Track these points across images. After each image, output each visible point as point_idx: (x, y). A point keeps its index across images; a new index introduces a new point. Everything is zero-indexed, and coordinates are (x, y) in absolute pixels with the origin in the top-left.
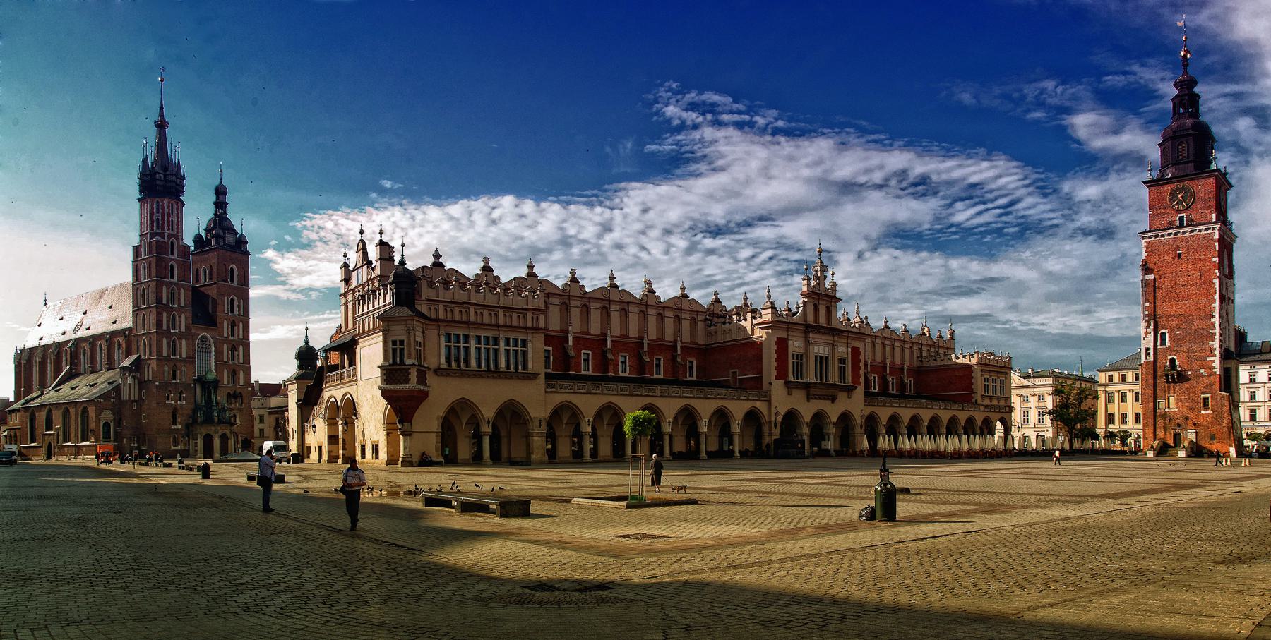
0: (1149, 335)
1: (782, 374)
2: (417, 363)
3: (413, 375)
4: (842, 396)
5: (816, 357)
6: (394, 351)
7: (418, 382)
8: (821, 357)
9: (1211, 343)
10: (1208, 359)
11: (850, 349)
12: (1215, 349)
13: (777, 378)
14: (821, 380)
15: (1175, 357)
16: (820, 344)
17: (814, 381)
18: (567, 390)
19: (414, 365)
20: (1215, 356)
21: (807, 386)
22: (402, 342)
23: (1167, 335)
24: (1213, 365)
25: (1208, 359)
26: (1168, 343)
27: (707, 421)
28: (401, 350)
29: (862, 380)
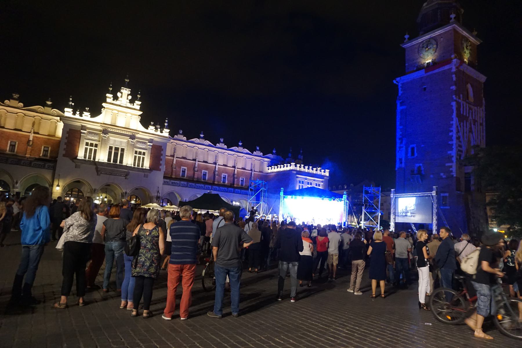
8: (117, 149)
9: (449, 152)
10: (447, 165)
12: (453, 156)
20: (452, 162)
24: (451, 169)
25: (447, 165)
26: (416, 155)
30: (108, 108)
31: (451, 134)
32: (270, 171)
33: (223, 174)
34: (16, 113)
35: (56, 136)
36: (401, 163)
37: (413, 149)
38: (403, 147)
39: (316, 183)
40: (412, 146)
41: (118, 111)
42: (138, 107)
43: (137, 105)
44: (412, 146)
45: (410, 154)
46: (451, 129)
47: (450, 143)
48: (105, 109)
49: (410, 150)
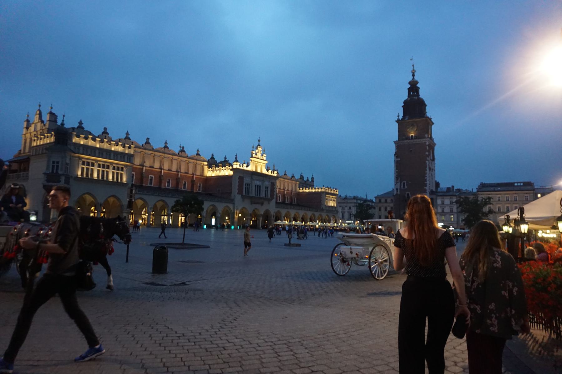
0: (398, 183)
1: (240, 192)
2: (65, 173)
3: (63, 179)
4: (266, 203)
5: (255, 186)
6: (53, 166)
7: (65, 183)
8: (258, 186)
9: (425, 188)
11: (270, 183)
12: (426, 190)
13: (238, 193)
14: (257, 195)
15: (409, 193)
16: (257, 180)
17: (254, 196)
18: (141, 193)
19: (63, 175)
21: (251, 198)
22: (58, 163)
23: (406, 184)
26: (406, 187)
27: (206, 211)
28: (57, 166)
29: (275, 197)
30: (254, 161)
31: (426, 178)
32: (301, 191)
33: (150, 176)
34: (176, 159)
35: (204, 176)
36: (397, 191)
37: (404, 184)
38: (398, 182)
39: (334, 199)
40: (404, 182)
41: (258, 162)
42: (265, 159)
43: (265, 157)
44: (404, 182)
45: (402, 187)
46: (426, 175)
47: (425, 183)
48: (252, 162)
49: (402, 184)
